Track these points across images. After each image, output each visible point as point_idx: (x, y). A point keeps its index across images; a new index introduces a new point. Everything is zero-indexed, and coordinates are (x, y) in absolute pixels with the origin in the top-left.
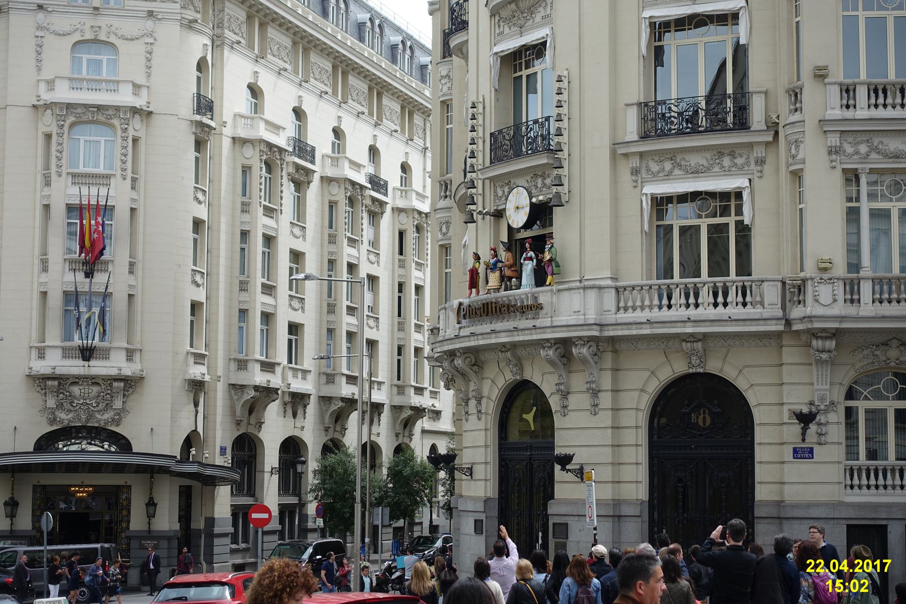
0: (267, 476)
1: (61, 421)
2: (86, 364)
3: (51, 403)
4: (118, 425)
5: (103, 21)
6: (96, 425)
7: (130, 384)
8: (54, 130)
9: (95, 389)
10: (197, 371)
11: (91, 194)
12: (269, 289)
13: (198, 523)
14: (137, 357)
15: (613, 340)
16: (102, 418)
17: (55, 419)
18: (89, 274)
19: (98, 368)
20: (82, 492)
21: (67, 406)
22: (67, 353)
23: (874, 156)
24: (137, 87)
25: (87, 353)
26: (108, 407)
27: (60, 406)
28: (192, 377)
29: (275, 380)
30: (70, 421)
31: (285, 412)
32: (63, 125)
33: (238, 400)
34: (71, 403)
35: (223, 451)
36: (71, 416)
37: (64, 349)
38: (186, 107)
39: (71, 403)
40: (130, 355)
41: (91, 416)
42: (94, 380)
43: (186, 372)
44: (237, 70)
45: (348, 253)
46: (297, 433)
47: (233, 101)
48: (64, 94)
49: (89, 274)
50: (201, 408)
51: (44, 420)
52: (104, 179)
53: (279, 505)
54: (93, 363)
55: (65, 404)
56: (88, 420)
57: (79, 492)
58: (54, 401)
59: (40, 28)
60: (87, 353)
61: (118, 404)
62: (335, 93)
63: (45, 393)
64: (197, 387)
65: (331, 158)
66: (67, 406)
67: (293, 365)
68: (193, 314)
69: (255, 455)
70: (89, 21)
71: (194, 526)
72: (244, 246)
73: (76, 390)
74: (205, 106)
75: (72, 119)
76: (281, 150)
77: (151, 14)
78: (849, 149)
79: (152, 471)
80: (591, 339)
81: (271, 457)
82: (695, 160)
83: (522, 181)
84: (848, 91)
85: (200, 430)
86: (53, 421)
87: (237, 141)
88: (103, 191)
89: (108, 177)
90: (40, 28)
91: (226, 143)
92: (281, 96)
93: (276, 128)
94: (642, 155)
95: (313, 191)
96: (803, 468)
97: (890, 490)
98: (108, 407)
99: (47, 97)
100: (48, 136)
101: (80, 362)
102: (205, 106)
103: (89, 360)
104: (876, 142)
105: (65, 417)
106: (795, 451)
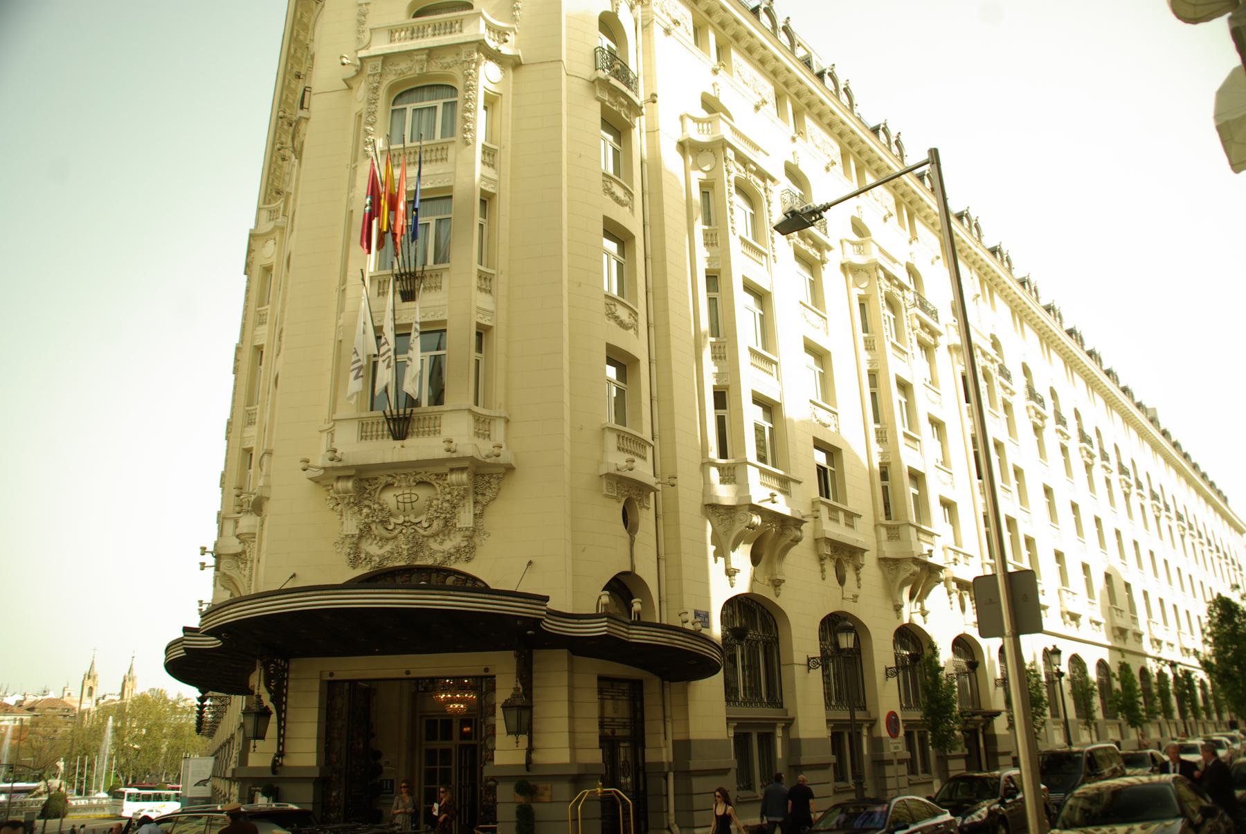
0: (799, 671)
1: (369, 558)
2: (398, 443)
3: (351, 525)
4: (468, 560)
6: (430, 562)
7: (486, 477)
13: (660, 752)
14: (498, 431)
16: (437, 552)
20: (460, 701)
25: (400, 427)
28: (612, 470)
30: (383, 558)
31: (823, 571)
32: (376, 88)
33: (725, 533)
34: (384, 522)
36: (388, 548)
37: (363, 424)
39: (384, 522)
40: (482, 424)
41: (418, 545)
43: (600, 462)
45: (895, 367)
46: (849, 608)
49: (408, 296)
51: (343, 561)
53: (828, 721)
54: (407, 442)
56: (414, 554)
57: (452, 701)
58: (355, 522)
61: (465, 518)
65: (853, 243)
66: (377, 530)
67: (831, 501)
68: (484, 213)
69: (777, 639)
71: (651, 756)
72: (713, 295)
73: (389, 498)
81: (803, 641)
86: (355, 560)
87: (688, 149)
98: (448, 526)
101: (391, 443)
105: (377, 552)
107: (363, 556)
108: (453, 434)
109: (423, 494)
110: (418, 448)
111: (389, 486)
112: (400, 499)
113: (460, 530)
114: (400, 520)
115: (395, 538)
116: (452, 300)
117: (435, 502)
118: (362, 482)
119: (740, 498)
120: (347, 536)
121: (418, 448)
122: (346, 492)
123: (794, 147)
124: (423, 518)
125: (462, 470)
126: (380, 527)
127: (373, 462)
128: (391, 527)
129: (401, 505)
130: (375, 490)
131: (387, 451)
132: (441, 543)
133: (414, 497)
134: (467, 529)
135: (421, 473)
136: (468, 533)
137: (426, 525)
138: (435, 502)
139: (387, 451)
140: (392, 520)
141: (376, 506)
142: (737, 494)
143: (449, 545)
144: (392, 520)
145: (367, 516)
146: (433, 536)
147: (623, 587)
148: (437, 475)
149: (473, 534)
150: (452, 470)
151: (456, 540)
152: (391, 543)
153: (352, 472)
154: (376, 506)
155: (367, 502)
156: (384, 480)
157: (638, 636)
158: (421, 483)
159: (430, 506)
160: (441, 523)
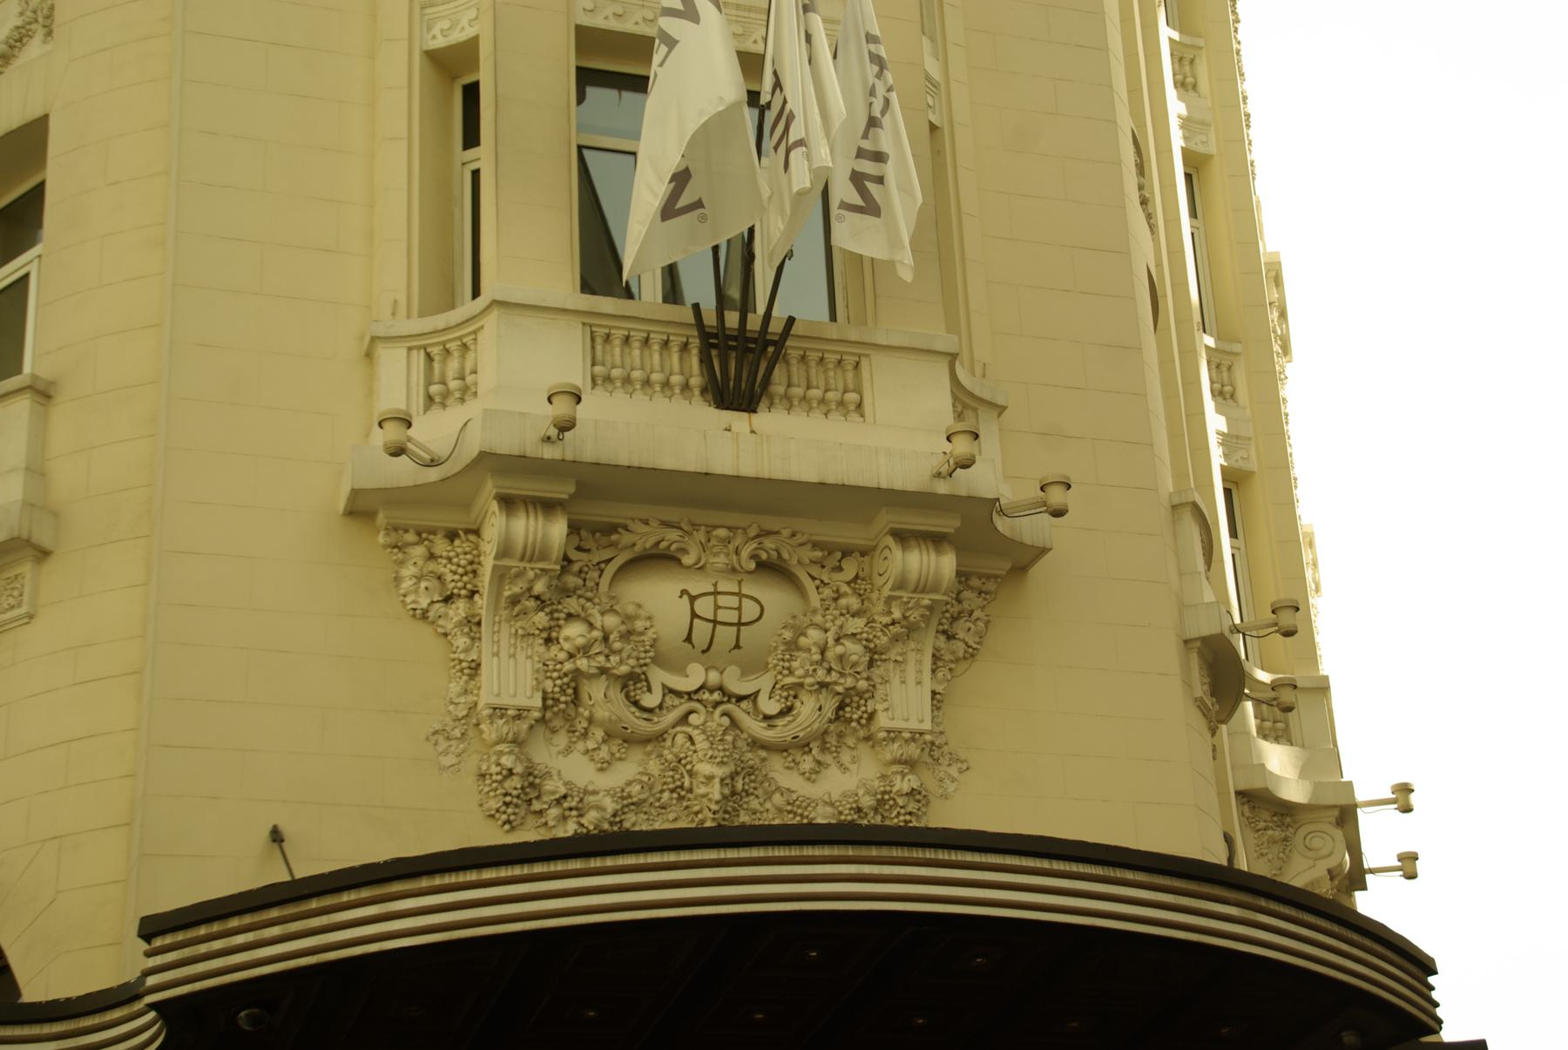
3: (512, 675)
17: (532, 781)
21: (602, 700)
25: (740, 361)
27: (561, 706)
30: (629, 804)
34: (631, 682)
36: (629, 771)
39: (631, 682)
54: (765, 419)
55: (596, 691)
63: (472, 623)
66: (602, 700)
73: (661, 601)
98: (850, 713)
103: (750, 407)
105: (593, 778)
107: (554, 786)
109: (775, 599)
110: (779, 443)
111: (659, 559)
112: (704, 607)
113: (893, 735)
114: (694, 677)
115: (660, 737)
117: (814, 635)
118: (605, 516)
119: (1318, 787)
120: (498, 711)
121: (779, 443)
122: (535, 554)
124: (764, 683)
125: (937, 540)
126: (617, 695)
127: (668, 462)
128: (650, 700)
129: (702, 631)
130: (600, 567)
131: (685, 433)
132: (811, 776)
133: (750, 611)
134: (916, 735)
135: (789, 528)
136: (913, 751)
137: (770, 706)
138: (814, 635)
139: (685, 433)
140: (658, 677)
141: (611, 621)
142: (1304, 773)
144: (658, 677)
145: (585, 650)
146: (781, 749)
148: (829, 549)
149: (928, 750)
150: (903, 537)
152: (637, 754)
153: (563, 490)
154: (611, 621)
155: (572, 604)
156: (644, 537)
158: (772, 569)
159: (792, 646)
160: (830, 705)
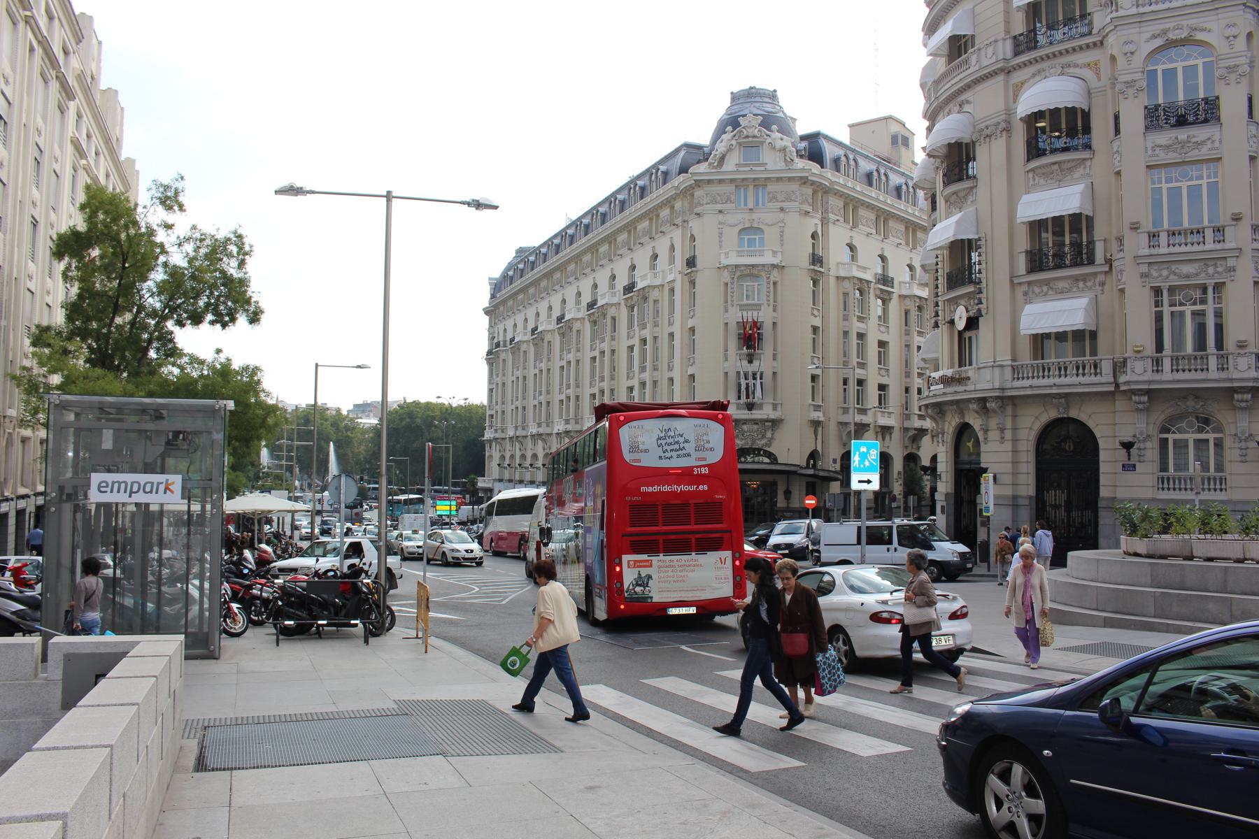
5: (755, 216)
7: (775, 423)
8: (728, 280)
9: (756, 427)
10: (818, 415)
11: (750, 316)
12: (862, 365)
14: (779, 407)
15: (1012, 398)
16: (760, 443)
18: (750, 362)
19: (757, 414)
22: (739, 407)
23: (1172, 277)
24: (775, 253)
25: (750, 407)
26: (763, 436)
29: (866, 419)
35: (835, 461)
38: (805, 262)
40: (775, 407)
41: (754, 442)
42: (755, 422)
44: (838, 236)
47: (836, 255)
48: (734, 260)
49: (750, 362)
50: (819, 437)
52: (757, 307)
59: (720, 223)
60: (750, 407)
61: (769, 435)
62: (907, 244)
64: (816, 424)
70: (747, 216)
73: (745, 427)
74: (816, 260)
75: (738, 273)
76: (868, 282)
77: (782, 209)
78: (1155, 274)
79: (790, 474)
80: (997, 397)
82: (1061, 284)
83: (963, 302)
84: (1153, 236)
85: (819, 449)
88: (755, 314)
89: (760, 305)
90: (720, 223)
91: (832, 281)
92: (870, 248)
93: (864, 269)
94: (1029, 283)
95: (894, 305)
96: (1129, 476)
97: (1189, 492)
98: (763, 436)
99: (725, 262)
100: (726, 284)
102: (816, 260)
104: (1173, 267)
106: (1124, 466)
108: (766, 412)
116: (764, 363)
121: (757, 414)
123: (883, 245)
143: (764, 442)
147: (813, 455)
149: (772, 439)
151: (764, 442)
157: (821, 474)
